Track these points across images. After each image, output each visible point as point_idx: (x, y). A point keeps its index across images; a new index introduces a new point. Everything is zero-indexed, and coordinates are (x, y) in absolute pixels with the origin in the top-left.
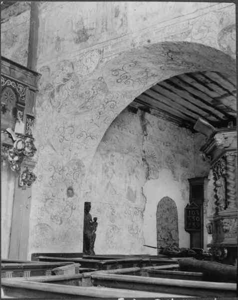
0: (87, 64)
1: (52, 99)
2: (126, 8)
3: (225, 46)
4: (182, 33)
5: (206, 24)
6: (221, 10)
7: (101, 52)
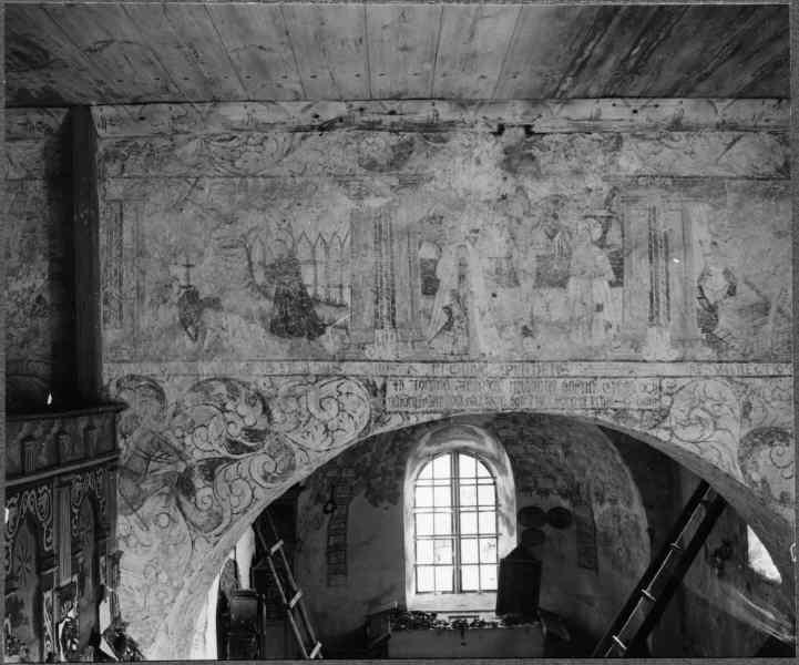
0: (324, 416)
1: (182, 499)
2: (462, 277)
3: (756, 477)
4: (643, 411)
5: (708, 405)
6: (747, 381)
7: (376, 391)
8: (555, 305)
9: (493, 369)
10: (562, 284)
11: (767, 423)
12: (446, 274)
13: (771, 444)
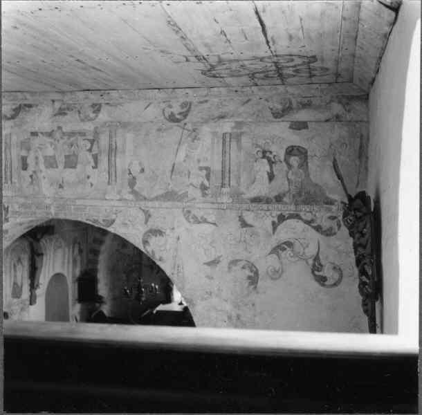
8: (69, 175)
9: (48, 201)
10: (75, 167)
11: (154, 228)
12: (31, 161)
13: (156, 236)
